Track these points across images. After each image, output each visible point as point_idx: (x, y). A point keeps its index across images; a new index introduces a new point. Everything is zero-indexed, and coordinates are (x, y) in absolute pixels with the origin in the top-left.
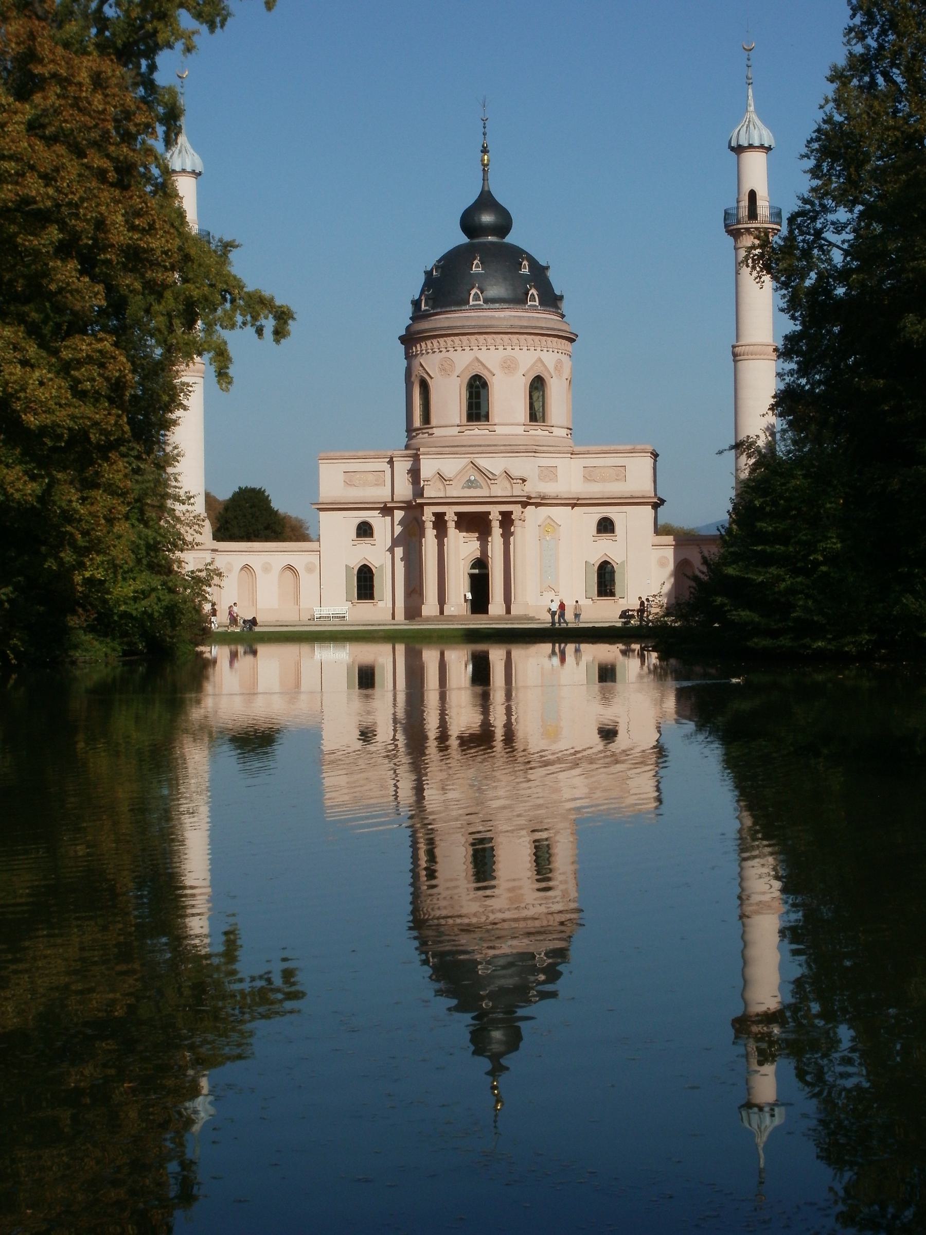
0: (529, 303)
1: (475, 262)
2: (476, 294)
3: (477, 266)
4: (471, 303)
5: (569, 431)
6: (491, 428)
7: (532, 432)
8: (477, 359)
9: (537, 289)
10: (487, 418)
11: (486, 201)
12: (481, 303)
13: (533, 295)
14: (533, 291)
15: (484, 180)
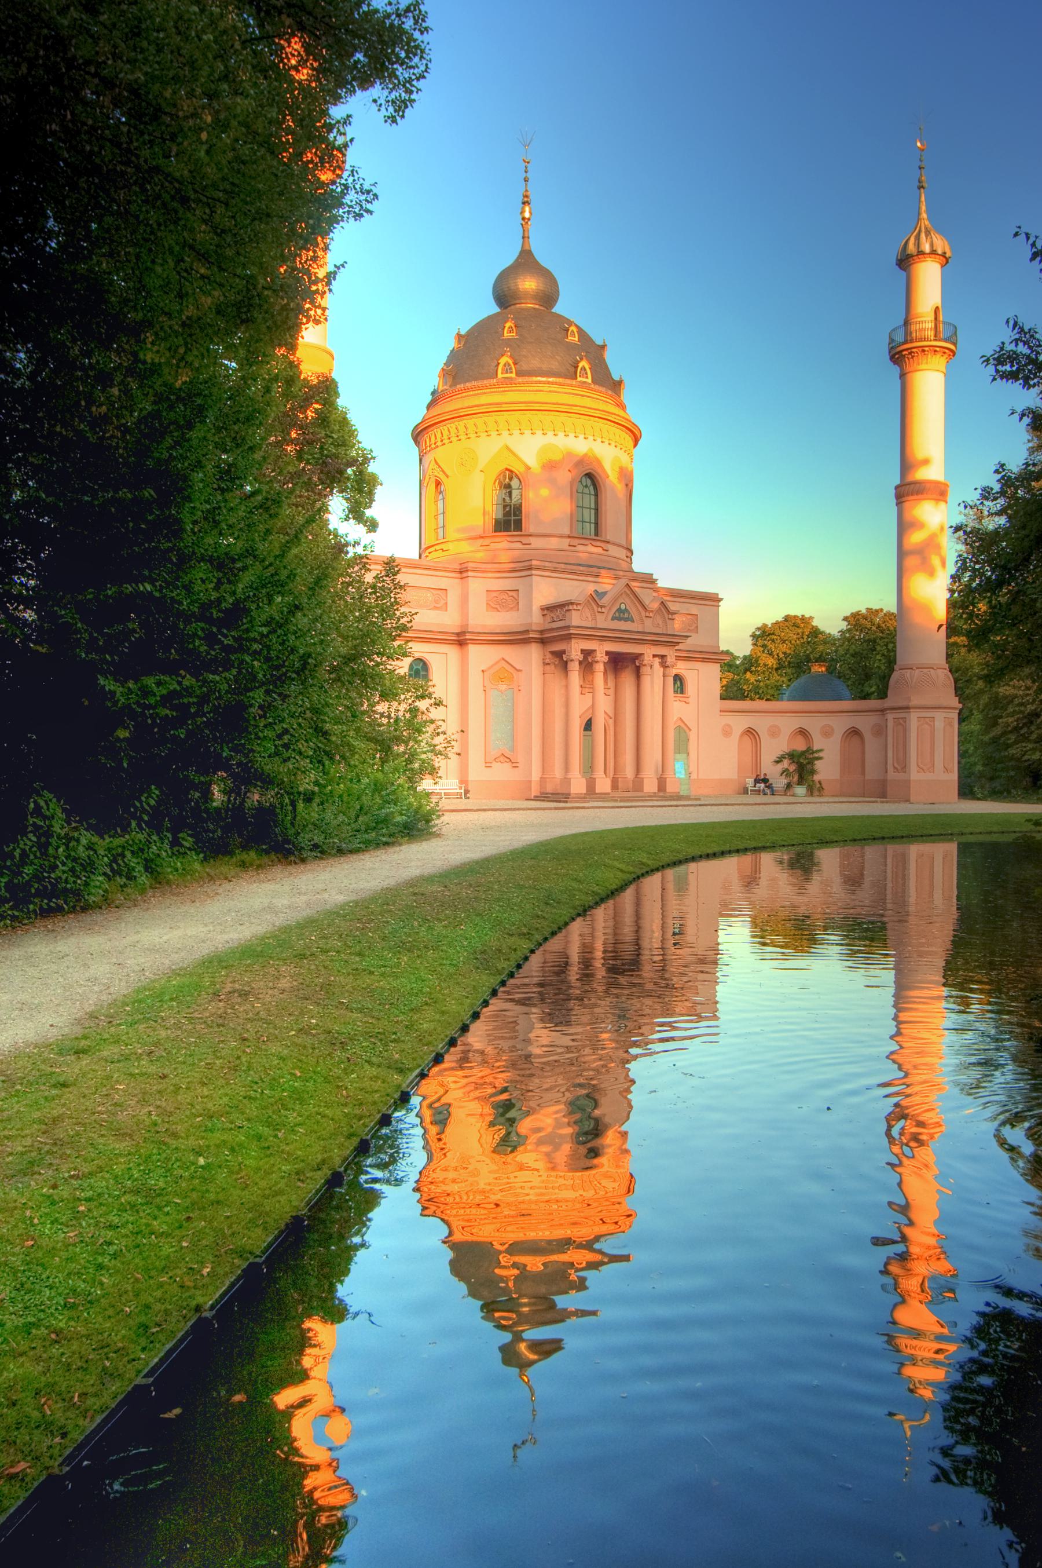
0: (579, 379)
1: (508, 325)
2: (507, 364)
3: (510, 331)
4: (500, 375)
5: (629, 554)
6: (525, 540)
7: (581, 548)
8: (508, 448)
9: (589, 363)
10: (518, 525)
11: (526, 261)
12: (513, 375)
13: (584, 368)
14: (584, 364)
15: (523, 237)
